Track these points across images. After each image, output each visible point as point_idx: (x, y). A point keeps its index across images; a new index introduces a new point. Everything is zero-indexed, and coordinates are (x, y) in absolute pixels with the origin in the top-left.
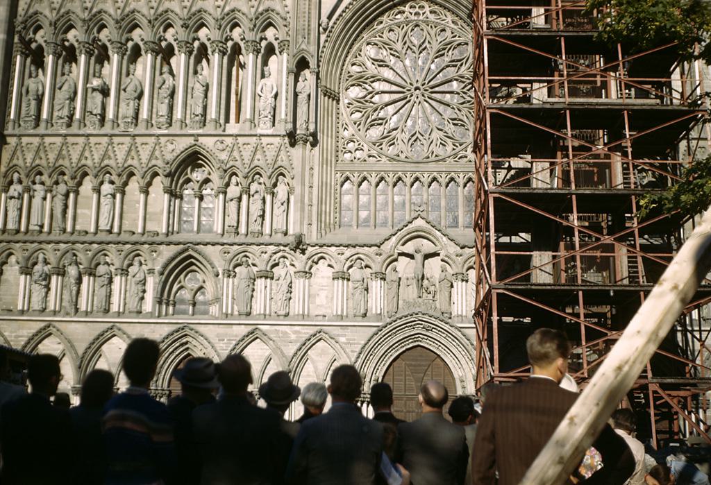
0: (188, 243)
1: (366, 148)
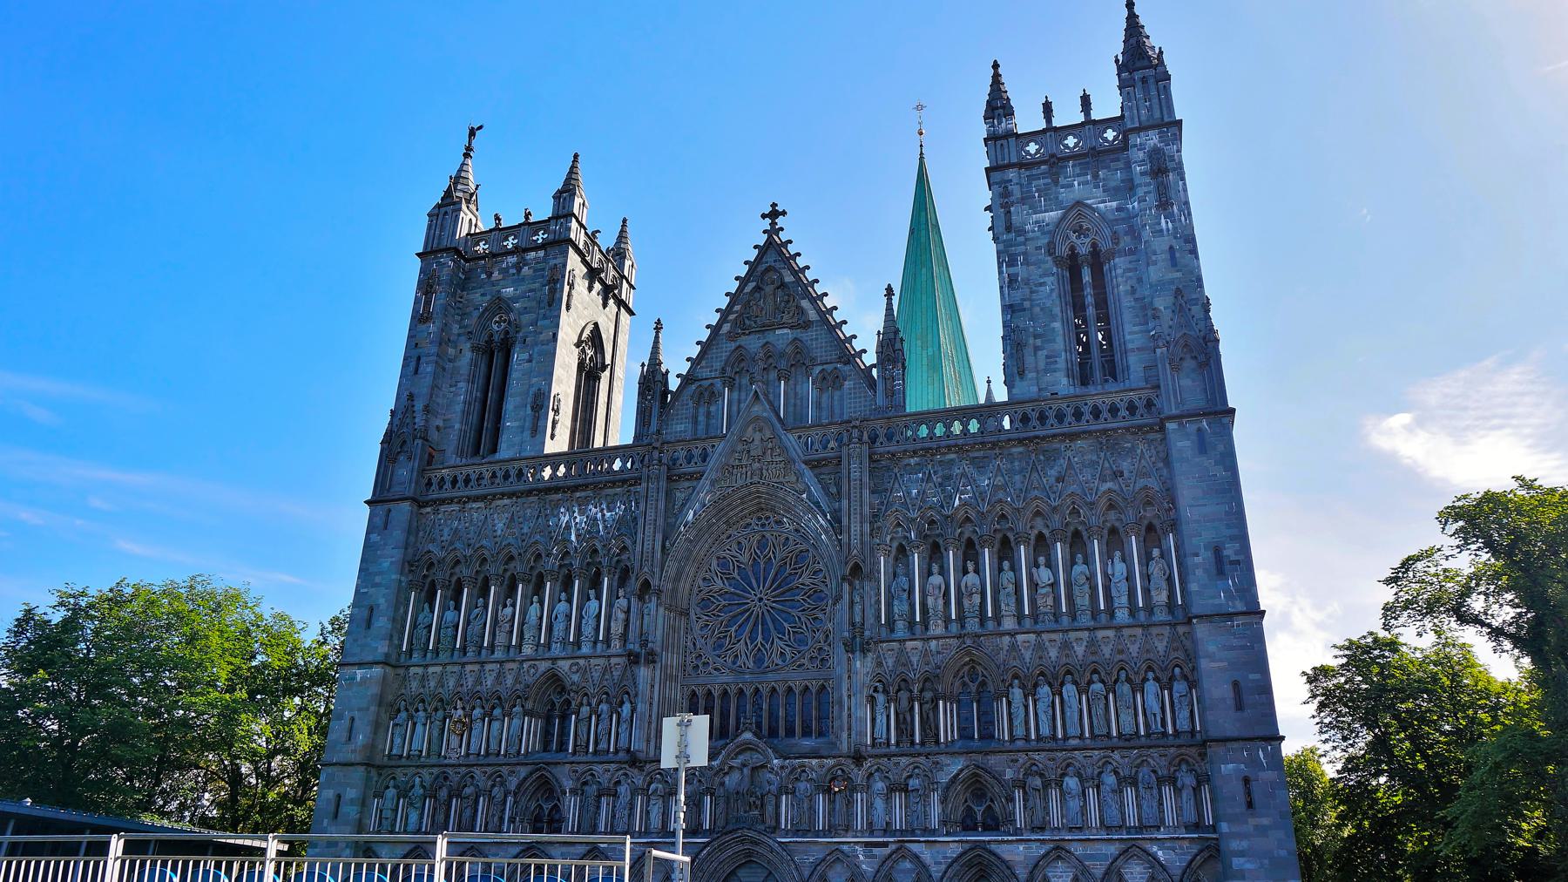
0: (540, 763)
1: (711, 661)
